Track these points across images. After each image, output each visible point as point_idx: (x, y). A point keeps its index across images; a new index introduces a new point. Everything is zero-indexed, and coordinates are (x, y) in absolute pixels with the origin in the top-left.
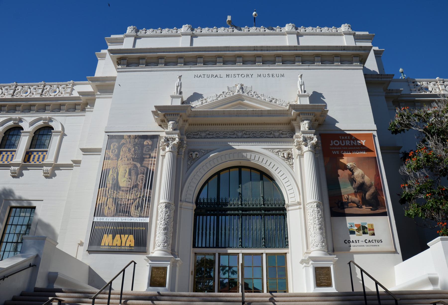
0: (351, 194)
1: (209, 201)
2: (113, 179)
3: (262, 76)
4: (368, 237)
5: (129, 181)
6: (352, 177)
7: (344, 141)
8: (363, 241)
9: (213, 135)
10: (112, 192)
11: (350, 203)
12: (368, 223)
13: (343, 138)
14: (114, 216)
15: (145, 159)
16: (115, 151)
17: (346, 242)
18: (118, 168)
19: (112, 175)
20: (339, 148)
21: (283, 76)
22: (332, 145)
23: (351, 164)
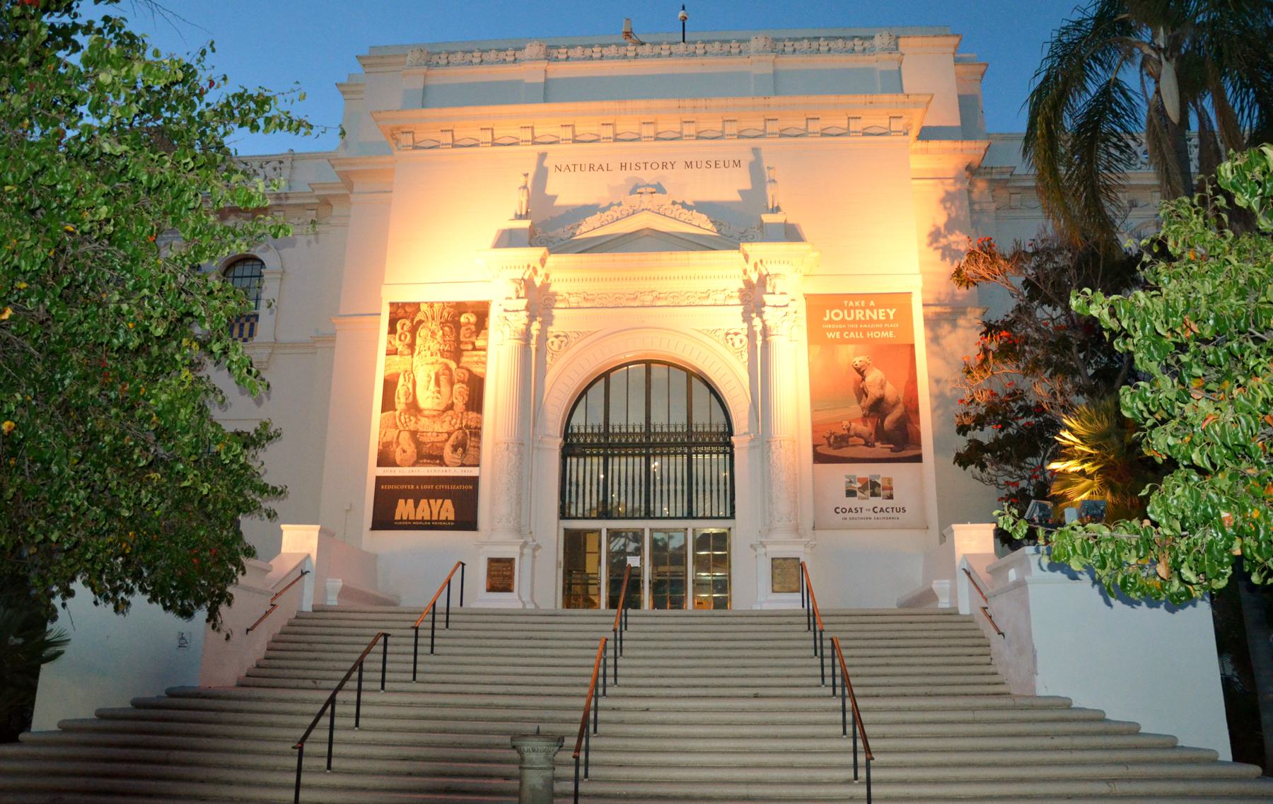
0: (856, 420)
1: (589, 430)
2: (407, 394)
3: (694, 164)
4: (879, 502)
9: (594, 300)
12: (882, 475)
13: (851, 304)
14: (414, 465)
15: (465, 353)
16: (406, 337)
20: (840, 326)
22: (827, 319)
23: (861, 358)
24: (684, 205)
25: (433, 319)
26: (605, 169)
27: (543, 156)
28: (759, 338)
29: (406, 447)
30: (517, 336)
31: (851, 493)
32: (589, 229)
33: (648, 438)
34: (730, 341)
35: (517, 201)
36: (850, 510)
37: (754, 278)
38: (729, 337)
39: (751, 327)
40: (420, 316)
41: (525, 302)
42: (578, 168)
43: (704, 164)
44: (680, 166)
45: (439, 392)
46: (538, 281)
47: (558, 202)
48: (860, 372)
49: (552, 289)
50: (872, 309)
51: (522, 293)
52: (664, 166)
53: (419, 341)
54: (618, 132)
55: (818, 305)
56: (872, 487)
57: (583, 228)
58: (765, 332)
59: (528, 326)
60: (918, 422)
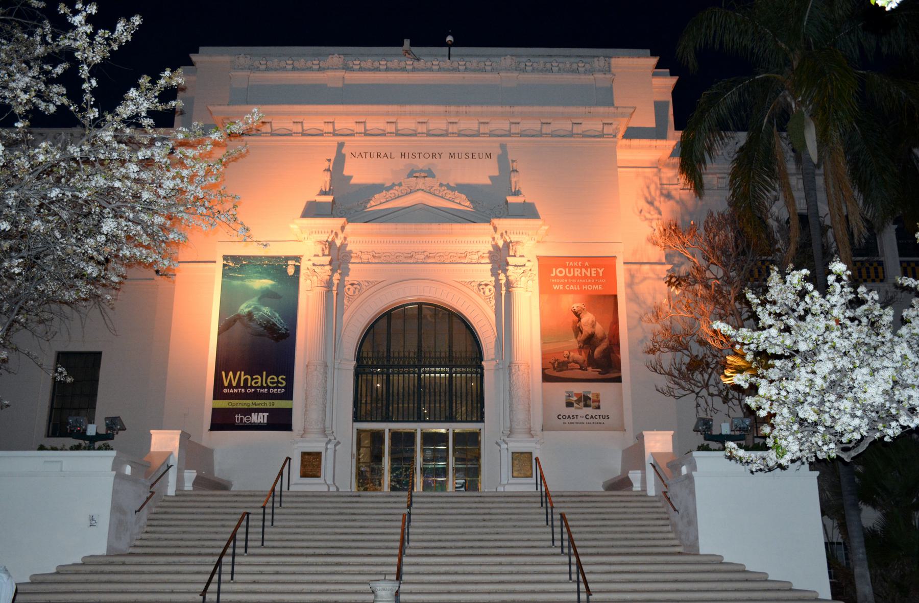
0: (573, 351)
3: (456, 155)
4: (590, 411)
6: (578, 325)
7: (572, 270)
8: (583, 417)
11: (571, 363)
12: (592, 392)
17: (560, 417)
22: (553, 275)
23: (578, 305)
24: (449, 187)
26: (389, 156)
27: (341, 145)
28: (504, 289)
30: (323, 285)
31: (569, 404)
32: (377, 203)
33: (420, 361)
34: (482, 290)
35: (324, 180)
36: (569, 417)
37: (501, 243)
38: (481, 287)
39: (497, 281)
41: (329, 258)
42: (368, 155)
43: (464, 155)
44: (446, 156)
46: (338, 242)
47: (353, 181)
48: (578, 315)
49: (348, 249)
50: (586, 268)
51: (327, 252)
52: (434, 156)
54: (399, 128)
55: (546, 264)
56: (585, 400)
57: (372, 203)
58: (509, 284)
59: (331, 277)
60: (619, 353)
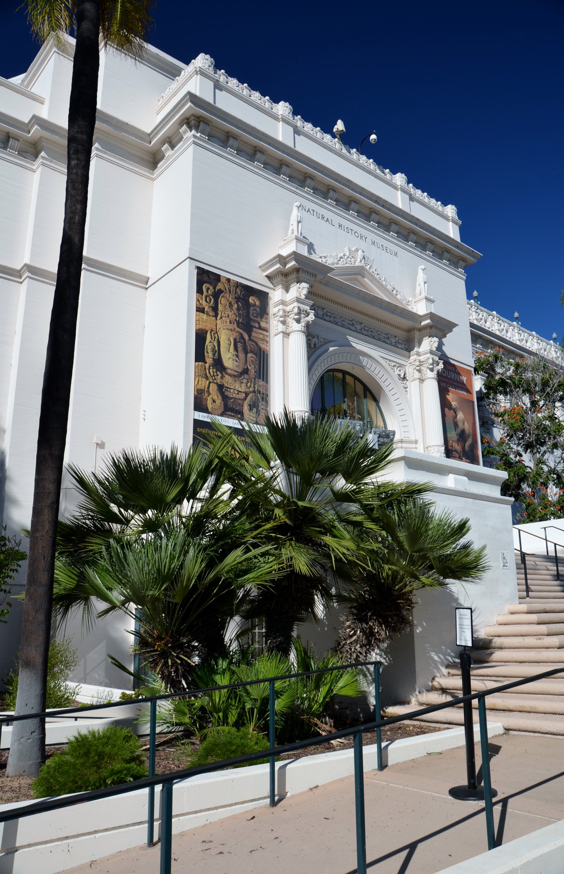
5: (236, 361)
10: (215, 374)
18: (219, 333)
19: (210, 342)
21: (396, 254)
25: (230, 292)
29: (215, 398)
40: (220, 286)
45: (237, 356)
53: (220, 307)
